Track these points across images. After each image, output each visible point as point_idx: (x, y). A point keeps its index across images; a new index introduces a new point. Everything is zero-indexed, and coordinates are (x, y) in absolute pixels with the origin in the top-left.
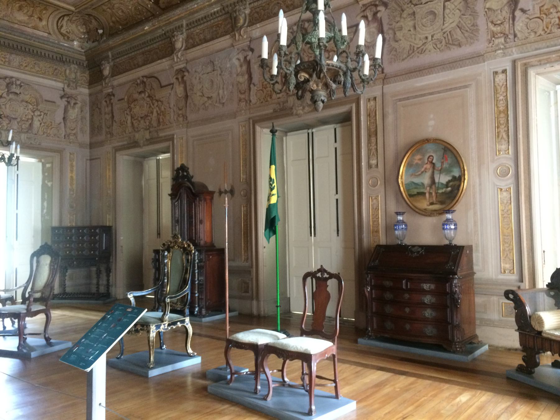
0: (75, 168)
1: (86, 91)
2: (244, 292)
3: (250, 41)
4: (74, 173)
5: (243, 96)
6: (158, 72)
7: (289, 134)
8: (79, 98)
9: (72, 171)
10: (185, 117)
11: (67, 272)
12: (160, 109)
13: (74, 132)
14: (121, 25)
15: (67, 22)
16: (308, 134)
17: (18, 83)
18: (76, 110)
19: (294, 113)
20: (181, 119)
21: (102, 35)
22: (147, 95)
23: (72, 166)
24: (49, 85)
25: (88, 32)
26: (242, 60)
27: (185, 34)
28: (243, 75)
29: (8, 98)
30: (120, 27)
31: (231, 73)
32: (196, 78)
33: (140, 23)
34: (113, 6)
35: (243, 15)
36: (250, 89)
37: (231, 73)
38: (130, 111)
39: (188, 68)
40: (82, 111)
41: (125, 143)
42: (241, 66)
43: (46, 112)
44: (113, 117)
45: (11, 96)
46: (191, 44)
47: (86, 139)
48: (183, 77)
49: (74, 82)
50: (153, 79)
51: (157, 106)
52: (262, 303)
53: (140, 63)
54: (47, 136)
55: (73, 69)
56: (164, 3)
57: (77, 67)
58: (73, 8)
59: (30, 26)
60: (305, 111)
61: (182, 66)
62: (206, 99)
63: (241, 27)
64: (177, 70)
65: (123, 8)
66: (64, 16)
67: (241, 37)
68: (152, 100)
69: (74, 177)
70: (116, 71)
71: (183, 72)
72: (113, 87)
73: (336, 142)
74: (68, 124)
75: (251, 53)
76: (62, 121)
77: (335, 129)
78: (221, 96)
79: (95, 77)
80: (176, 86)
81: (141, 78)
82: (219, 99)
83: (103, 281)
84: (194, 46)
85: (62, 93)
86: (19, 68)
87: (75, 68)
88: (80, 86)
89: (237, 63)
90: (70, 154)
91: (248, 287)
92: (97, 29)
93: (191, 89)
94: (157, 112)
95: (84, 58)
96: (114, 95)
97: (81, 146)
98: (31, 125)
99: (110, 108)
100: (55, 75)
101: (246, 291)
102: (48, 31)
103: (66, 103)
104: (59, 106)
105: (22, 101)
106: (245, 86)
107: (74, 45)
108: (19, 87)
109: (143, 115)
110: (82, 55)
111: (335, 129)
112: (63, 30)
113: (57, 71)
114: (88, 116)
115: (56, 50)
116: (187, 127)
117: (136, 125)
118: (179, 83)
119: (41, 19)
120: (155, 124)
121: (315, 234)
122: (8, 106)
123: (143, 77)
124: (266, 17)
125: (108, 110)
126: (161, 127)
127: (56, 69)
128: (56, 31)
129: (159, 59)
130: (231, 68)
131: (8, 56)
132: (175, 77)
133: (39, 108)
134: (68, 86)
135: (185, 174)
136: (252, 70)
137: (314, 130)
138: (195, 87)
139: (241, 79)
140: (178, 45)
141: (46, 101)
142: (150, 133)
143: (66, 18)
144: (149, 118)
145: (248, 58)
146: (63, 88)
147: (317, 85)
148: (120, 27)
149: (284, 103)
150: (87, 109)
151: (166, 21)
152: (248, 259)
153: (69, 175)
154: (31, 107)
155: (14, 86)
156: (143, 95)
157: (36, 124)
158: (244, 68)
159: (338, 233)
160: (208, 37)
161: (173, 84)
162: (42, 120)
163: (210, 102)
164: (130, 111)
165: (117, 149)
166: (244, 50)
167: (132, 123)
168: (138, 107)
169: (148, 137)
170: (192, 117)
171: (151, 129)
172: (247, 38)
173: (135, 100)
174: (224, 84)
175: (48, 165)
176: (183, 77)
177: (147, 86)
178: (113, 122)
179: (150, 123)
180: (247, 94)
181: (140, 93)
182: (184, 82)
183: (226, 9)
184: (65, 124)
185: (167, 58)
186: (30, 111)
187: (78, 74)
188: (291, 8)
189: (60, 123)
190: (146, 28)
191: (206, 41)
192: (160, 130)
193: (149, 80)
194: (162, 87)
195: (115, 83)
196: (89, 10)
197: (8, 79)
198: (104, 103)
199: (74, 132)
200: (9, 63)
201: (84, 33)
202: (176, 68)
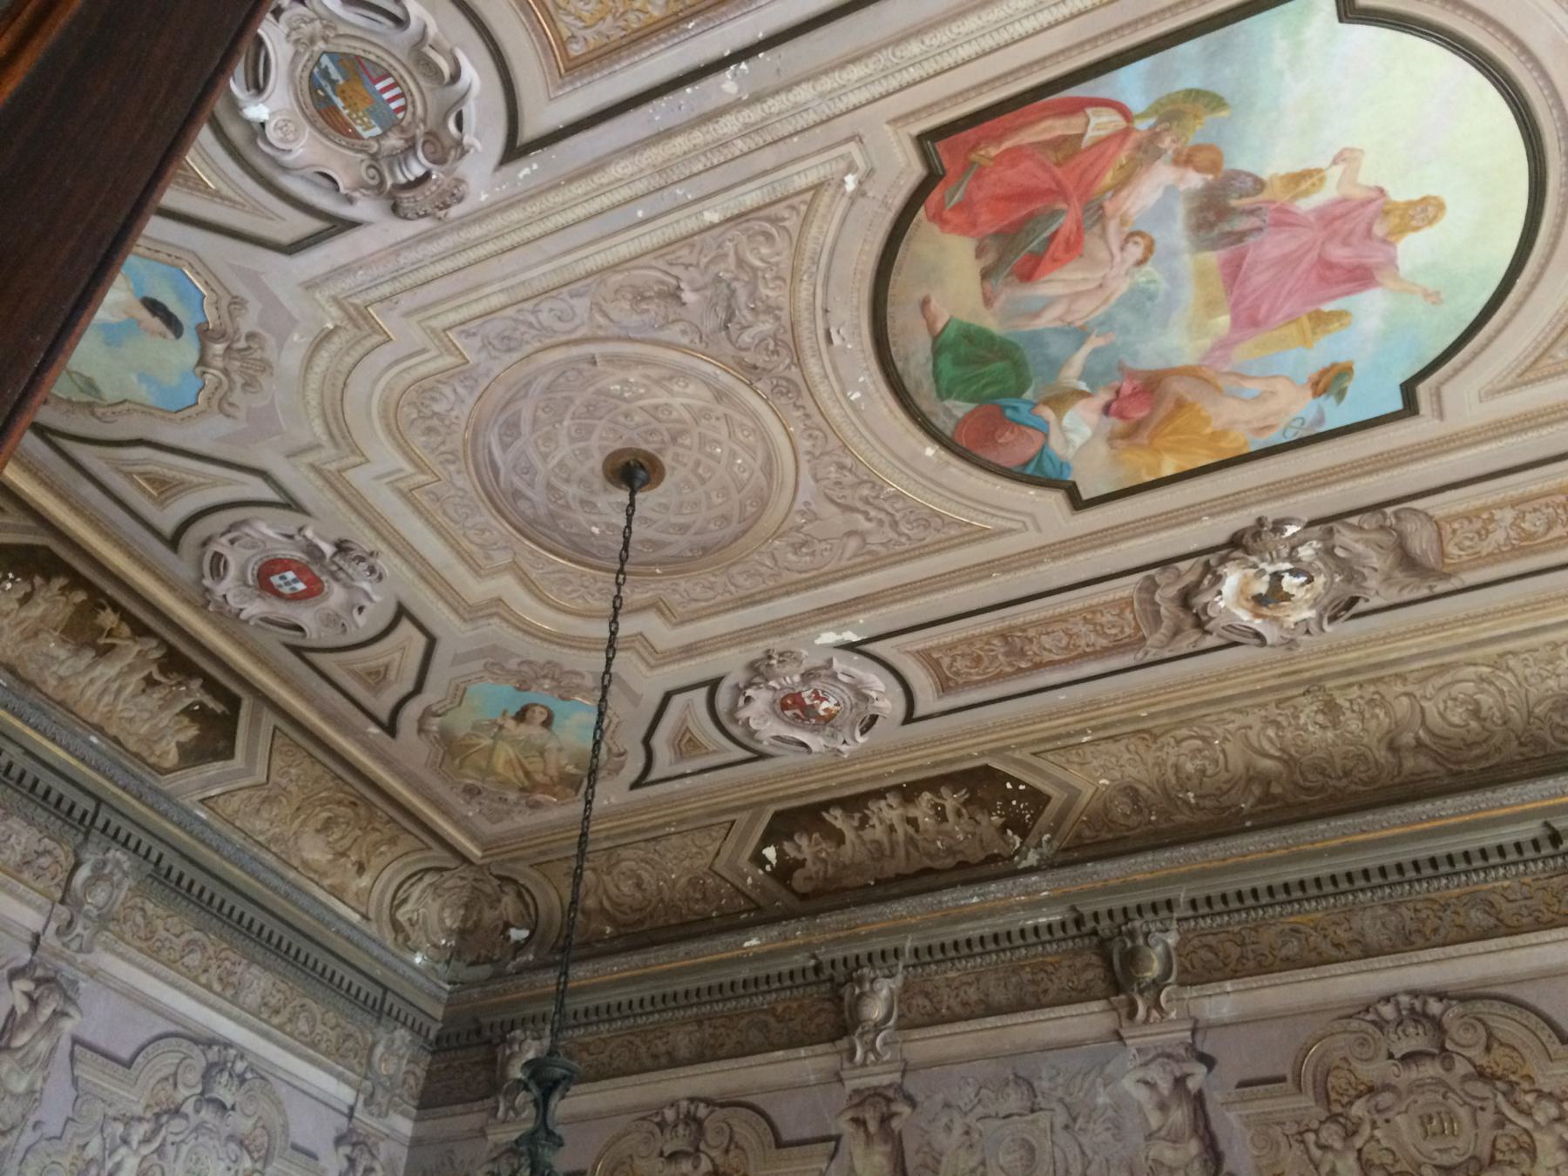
1: (405, 1126)
3: (1194, 1031)
6: (766, 1090)
8: (384, 1149)
14: (612, 920)
15: (423, 891)
17: (240, 1066)
21: (519, 947)
25: (462, 933)
26: (1165, 1087)
27: (900, 977)
28: (1175, 1140)
30: (608, 930)
31: (1117, 1126)
32: (948, 1128)
33: (732, 924)
34: (618, 862)
35: (1159, 948)
37: (1117, 1126)
39: (911, 1086)
42: (1163, 1107)
45: (207, 1114)
46: (918, 1014)
48: (885, 1120)
53: (683, 1052)
55: (398, 1043)
56: (810, 878)
59: (327, 882)
61: (886, 1080)
63: (1158, 985)
64: (856, 1091)
65: (645, 876)
66: (427, 870)
67: (1155, 1014)
71: (889, 1101)
75: (1204, 1069)
80: (854, 1145)
81: (684, 1104)
84: (935, 1019)
86: (264, 1015)
87: (403, 1037)
89: (1141, 1094)
92: (507, 925)
93: (925, 1166)
95: (439, 1012)
100: (337, 1054)
102: (363, 909)
103: (345, 1164)
105: (231, 1138)
108: (236, 1081)
110: (437, 999)
112: (402, 915)
113: (350, 1044)
115: (378, 972)
119: (361, 868)
122: (185, 1149)
123: (692, 1100)
124: (1251, 964)
127: (349, 1036)
128: (386, 912)
130: (1117, 1108)
131: (239, 969)
132: (849, 1115)
134: (367, 1103)
136: (1214, 1126)
138: (944, 1160)
139: (1168, 1154)
140: (875, 1010)
141: (295, 1147)
143: (428, 879)
145: (1192, 1085)
146: (352, 1109)
148: (608, 930)
151: (837, 930)
155: (226, 1075)
158: (1179, 1115)
160: (999, 997)
161: (837, 1139)
166: (1169, 1056)
172: (1178, 1020)
176: (885, 1120)
177: (710, 1135)
181: (674, 1157)
183: (1090, 925)
185: (820, 1048)
188: (1356, 951)
190: (754, 942)
191: (991, 1010)
193: (720, 1113)
194: (780, 1144)
196: (521, 866)
197: (216, 1048)
201: (449, 933)
202: (851, 1085)
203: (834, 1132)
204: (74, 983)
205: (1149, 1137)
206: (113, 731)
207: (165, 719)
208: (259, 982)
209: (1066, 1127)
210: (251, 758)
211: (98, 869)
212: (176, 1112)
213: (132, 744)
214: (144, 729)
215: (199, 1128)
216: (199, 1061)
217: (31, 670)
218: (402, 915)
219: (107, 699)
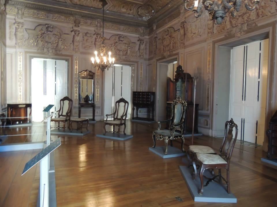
0: (142, 69)
1: (147, 37)
2: (206, 125)
4: (142, 71)
5: (210, 31)
7: (234, 48)
8: (145, 40)
9: (141, 70)
10: (184, 44)
11: (138, 109)
12: (174, 41)
13: (142, 54)
16: (245, 47)
17: (123, 36)
18: (144, 45)
19: (236, 36)
20: (182, 45)
21: (153, 13)
22: (169, 35)
23: (141, 68)
24: (134, 36)
29: (119, 43)
30: (160, 8)
32: (189, 25)
36: (213, 27)
38: (163, 44)
40: (146, 45)
41: (160, 57)
43: (132, 47)
44: (156, 47)
45: (120, 42)
47: (147, 57)
48: (183, 26)
49: (143, 34)
50: (172, 28)
51: (173, 40)
52: (214, 132)
54: (133, 56)
57: (144, 27)
58: (142, 3)
59: (127, 13)
60: (242, 34)
62: (193, 34)
64: (181, 23)
66: (139, 7)
68: (171, 38)
69: (142, 72)
70: (158, 27)
71: (184, 23)
72: (157, 34)
73: (260, 50)
74: (141, 51)
76: (138, 50)
77: (260, 43)
78: (199, 32)
79: (151, 31)
81: (167, 29)
82: (199, 34)
83: (151, 114)
85: (138, 39)
88: (145, 35)
90: (141, 63)
91: (208, 123)
92: (152, 10)
94: (173, 43)
96: (157, 38)
97: (145, 60)
98: (127, 52)
99: (155, 43)
100: (136, 32)
101: (207, 125)
103: (140, 43)
104: (137, 44)
106: (211, 26)
107: (143, 19)
109: (167, 45)
111: (260, 43)
112: (139, 13)
114: (148, 47)
115: (136, 21)
116: (184, 49)
117: (165, 49)
118: (182, 28)
119: (131, 10)
120: (171, 48)
121: (245, 100)
122: (119, 46)
123: (168, 28)
125: (155, 44)
126: (174, 49)
129: (174, 19)
133: (130, 45)
135: (181, 69)
137: (248, 45)
141: (133, 43)
142: (170, 52)
143: (140, 8)
144: (169, 46)
146: (139, 37)
147: (218, 8)
149: (231, 31)
150: (148, 45)
152: (208, 110)
153: (140, 71)
154: (127, 45)
156: (167, 36)
157: (129, 52)
159: (258, 100)
161: (179, 29)
162: (131, 50)
163: (194, 35)
164: (163, 44)
165: (157, 60)
167: (163, 49)
168: (165, 42)
169: (169, 54)
170: (187, 43)
171: (170, 51)
173: (165, 38)
174: (201, 26)
175: (133, 68)
176: (183, 26)
178: (156, 49)
179: (170, 48)
180: (212, 30)
181: (167, 35)
182: (184, 28)
184: (139, 51)
186: (126, 47)
187: (145, 30)
189: (137, 51)
190: (169, 6)
192: (173, 51)
193: (170, 29)
194: (175, 31)
195: (158, 32)
198: (154, 41)
199: (142, 54)
200: (119, 29)
202: (181, 22)
203: (179, 28)
204: (100, 33)
205: (208, 20)
206: (94, 7)
207: (98, 3)
208: (122, 27)
209: (200, 22)
210: (109, 3)
211: (97, 21)
212: (117, 42)
213: (96, 7)
214: (97, 5)
215: (120, 43)
216: (117, 37)
217: (82, 4)
218: (139, 13)
219: (91, 3)
